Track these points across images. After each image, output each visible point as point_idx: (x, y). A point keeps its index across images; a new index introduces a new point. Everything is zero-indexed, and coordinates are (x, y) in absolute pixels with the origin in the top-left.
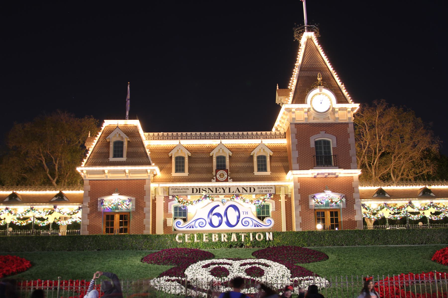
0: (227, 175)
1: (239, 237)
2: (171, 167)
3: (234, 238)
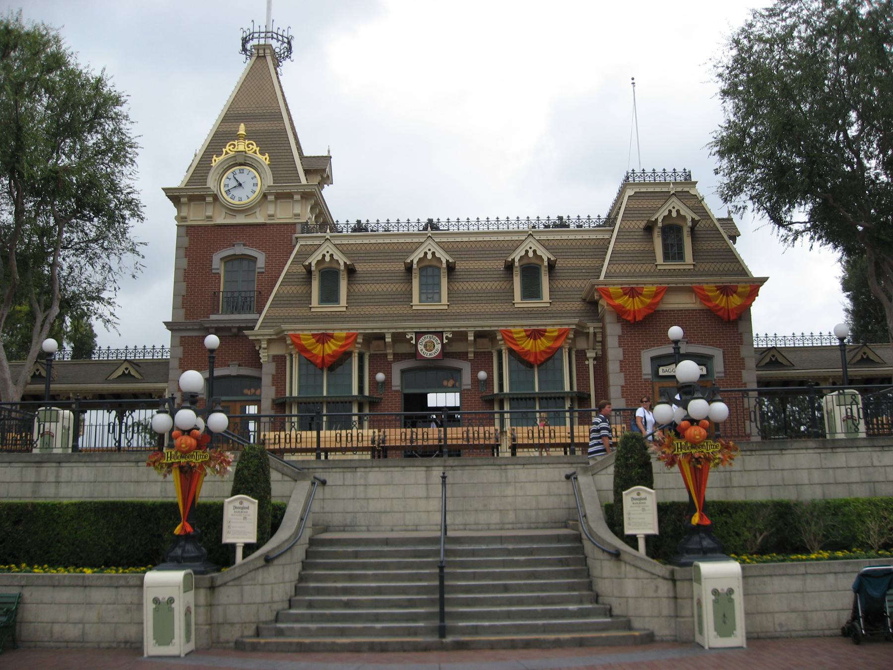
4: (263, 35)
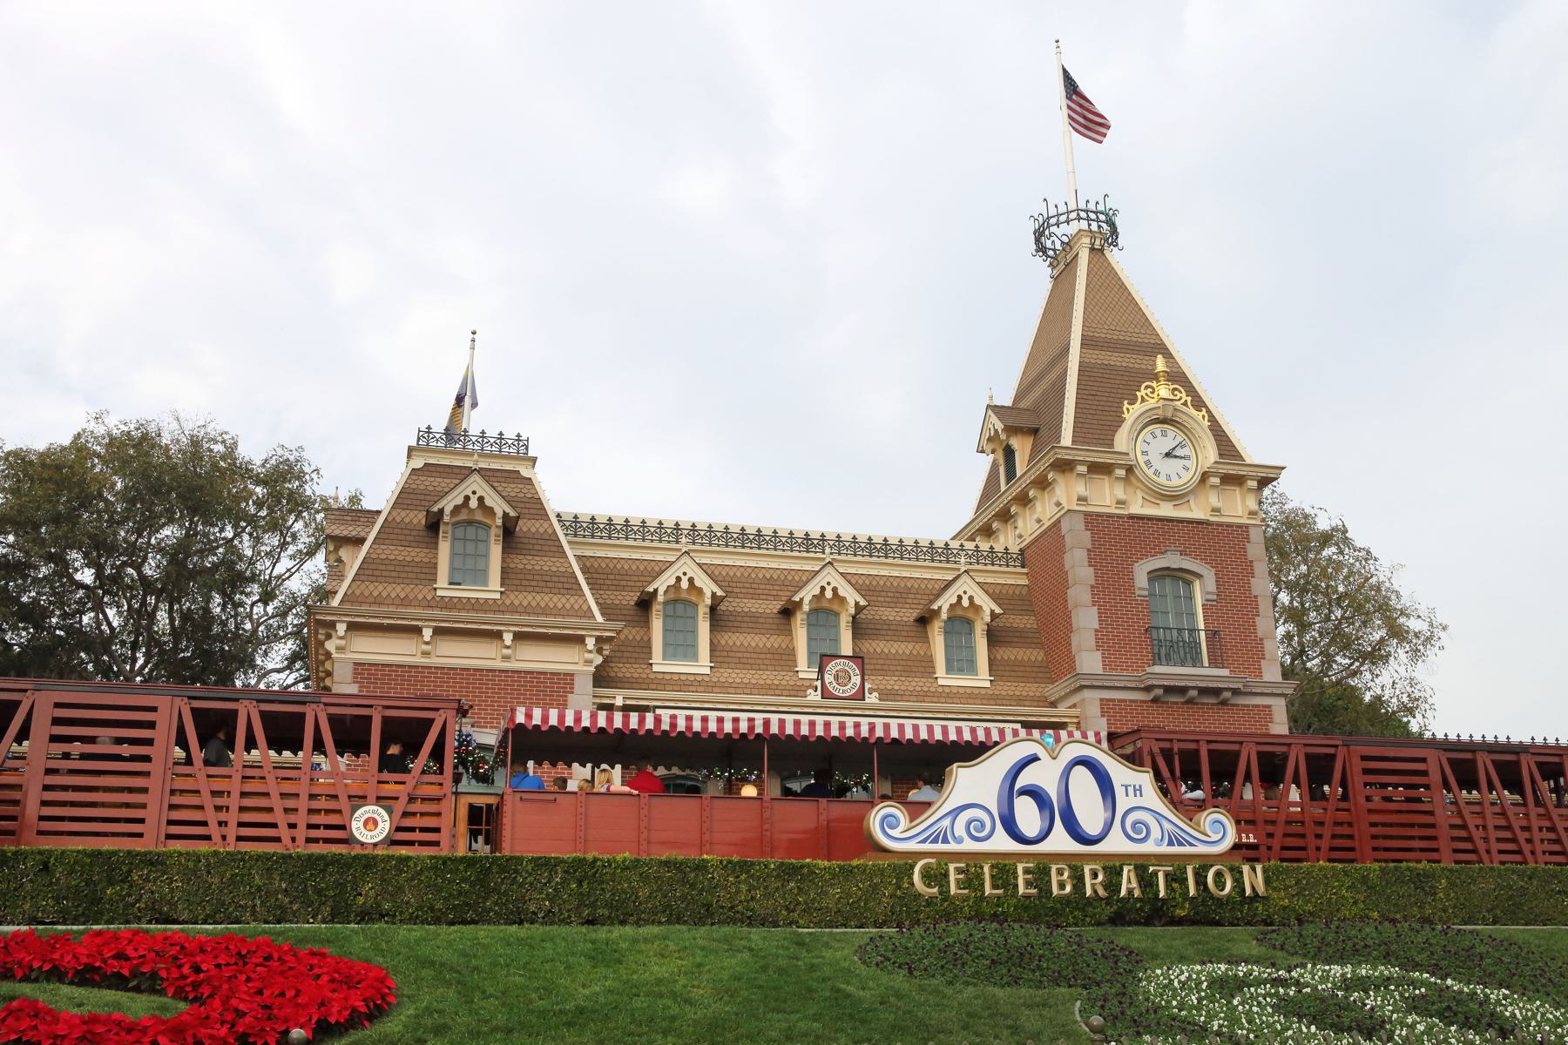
0: (859, 678)
1: (1147, 881)
2: (645, 639)
3: (1128, 882)
4: (1074, 215)
